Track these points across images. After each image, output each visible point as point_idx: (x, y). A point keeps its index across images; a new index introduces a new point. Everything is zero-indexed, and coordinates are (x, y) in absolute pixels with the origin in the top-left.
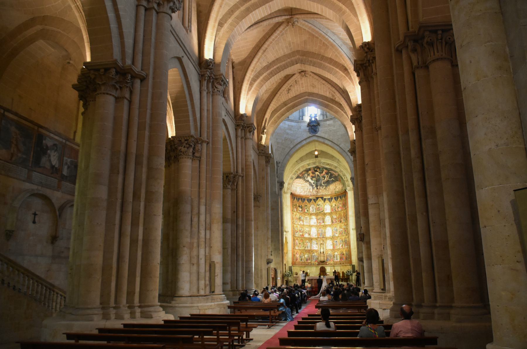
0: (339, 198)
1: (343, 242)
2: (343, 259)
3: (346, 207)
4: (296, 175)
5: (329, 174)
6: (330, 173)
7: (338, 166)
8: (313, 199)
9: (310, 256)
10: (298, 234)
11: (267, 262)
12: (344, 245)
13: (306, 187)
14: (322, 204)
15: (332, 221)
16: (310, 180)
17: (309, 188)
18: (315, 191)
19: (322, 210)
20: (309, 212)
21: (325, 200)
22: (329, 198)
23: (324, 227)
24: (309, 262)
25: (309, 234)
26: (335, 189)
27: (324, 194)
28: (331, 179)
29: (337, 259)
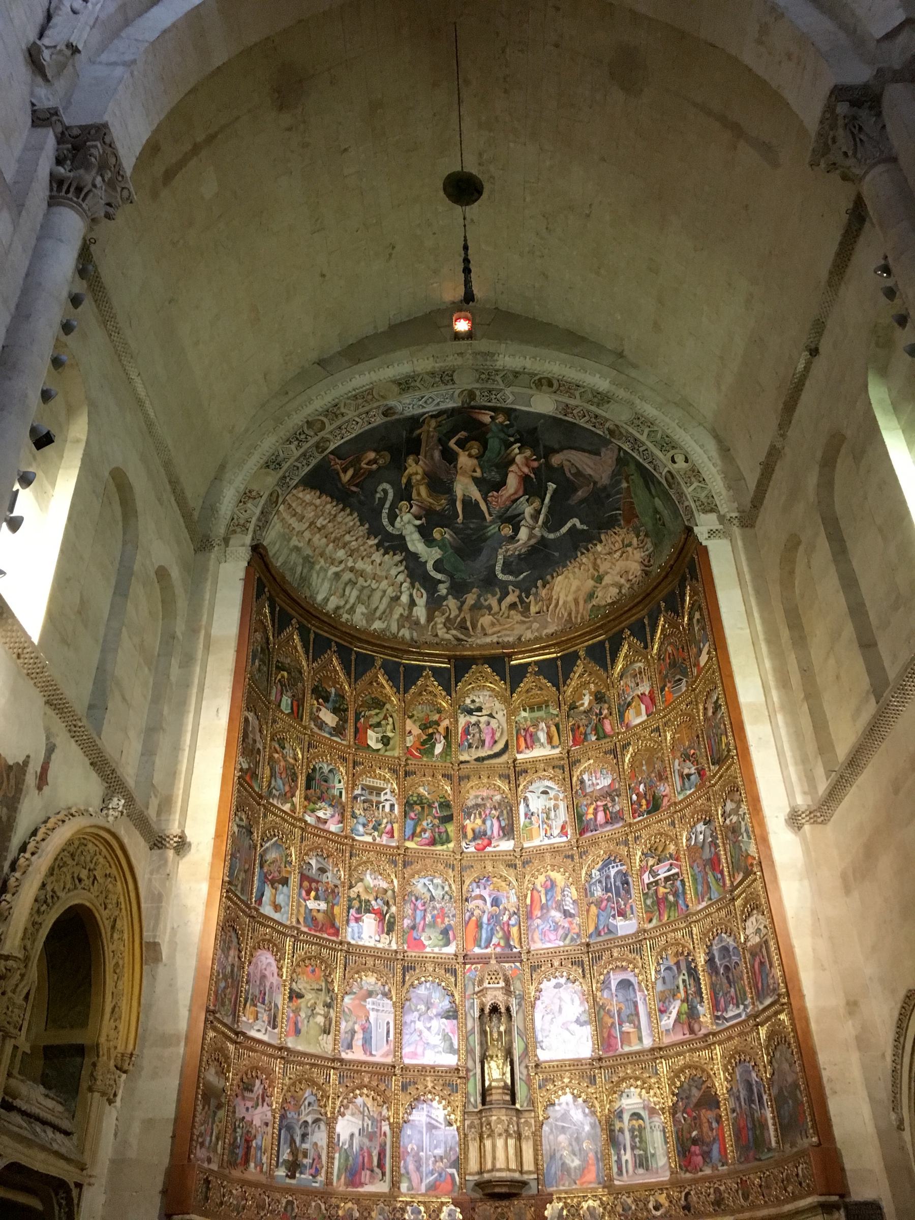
2: (706, 1155)
4: (306, 446)
5: (552, 486)
7: (621, 393)
8: (431, 668)
9: (386, 1128)
12: (704, 1011)
13: (384, 583)
16: (416, 544)
17: (404, 599)
19: (495, 742)
20: (396, 753)
21: (515, 676)
22: (556, 659)
23: (515, 866)
27: (511, 639)
28: (564, 530)
29: (643, 1162)
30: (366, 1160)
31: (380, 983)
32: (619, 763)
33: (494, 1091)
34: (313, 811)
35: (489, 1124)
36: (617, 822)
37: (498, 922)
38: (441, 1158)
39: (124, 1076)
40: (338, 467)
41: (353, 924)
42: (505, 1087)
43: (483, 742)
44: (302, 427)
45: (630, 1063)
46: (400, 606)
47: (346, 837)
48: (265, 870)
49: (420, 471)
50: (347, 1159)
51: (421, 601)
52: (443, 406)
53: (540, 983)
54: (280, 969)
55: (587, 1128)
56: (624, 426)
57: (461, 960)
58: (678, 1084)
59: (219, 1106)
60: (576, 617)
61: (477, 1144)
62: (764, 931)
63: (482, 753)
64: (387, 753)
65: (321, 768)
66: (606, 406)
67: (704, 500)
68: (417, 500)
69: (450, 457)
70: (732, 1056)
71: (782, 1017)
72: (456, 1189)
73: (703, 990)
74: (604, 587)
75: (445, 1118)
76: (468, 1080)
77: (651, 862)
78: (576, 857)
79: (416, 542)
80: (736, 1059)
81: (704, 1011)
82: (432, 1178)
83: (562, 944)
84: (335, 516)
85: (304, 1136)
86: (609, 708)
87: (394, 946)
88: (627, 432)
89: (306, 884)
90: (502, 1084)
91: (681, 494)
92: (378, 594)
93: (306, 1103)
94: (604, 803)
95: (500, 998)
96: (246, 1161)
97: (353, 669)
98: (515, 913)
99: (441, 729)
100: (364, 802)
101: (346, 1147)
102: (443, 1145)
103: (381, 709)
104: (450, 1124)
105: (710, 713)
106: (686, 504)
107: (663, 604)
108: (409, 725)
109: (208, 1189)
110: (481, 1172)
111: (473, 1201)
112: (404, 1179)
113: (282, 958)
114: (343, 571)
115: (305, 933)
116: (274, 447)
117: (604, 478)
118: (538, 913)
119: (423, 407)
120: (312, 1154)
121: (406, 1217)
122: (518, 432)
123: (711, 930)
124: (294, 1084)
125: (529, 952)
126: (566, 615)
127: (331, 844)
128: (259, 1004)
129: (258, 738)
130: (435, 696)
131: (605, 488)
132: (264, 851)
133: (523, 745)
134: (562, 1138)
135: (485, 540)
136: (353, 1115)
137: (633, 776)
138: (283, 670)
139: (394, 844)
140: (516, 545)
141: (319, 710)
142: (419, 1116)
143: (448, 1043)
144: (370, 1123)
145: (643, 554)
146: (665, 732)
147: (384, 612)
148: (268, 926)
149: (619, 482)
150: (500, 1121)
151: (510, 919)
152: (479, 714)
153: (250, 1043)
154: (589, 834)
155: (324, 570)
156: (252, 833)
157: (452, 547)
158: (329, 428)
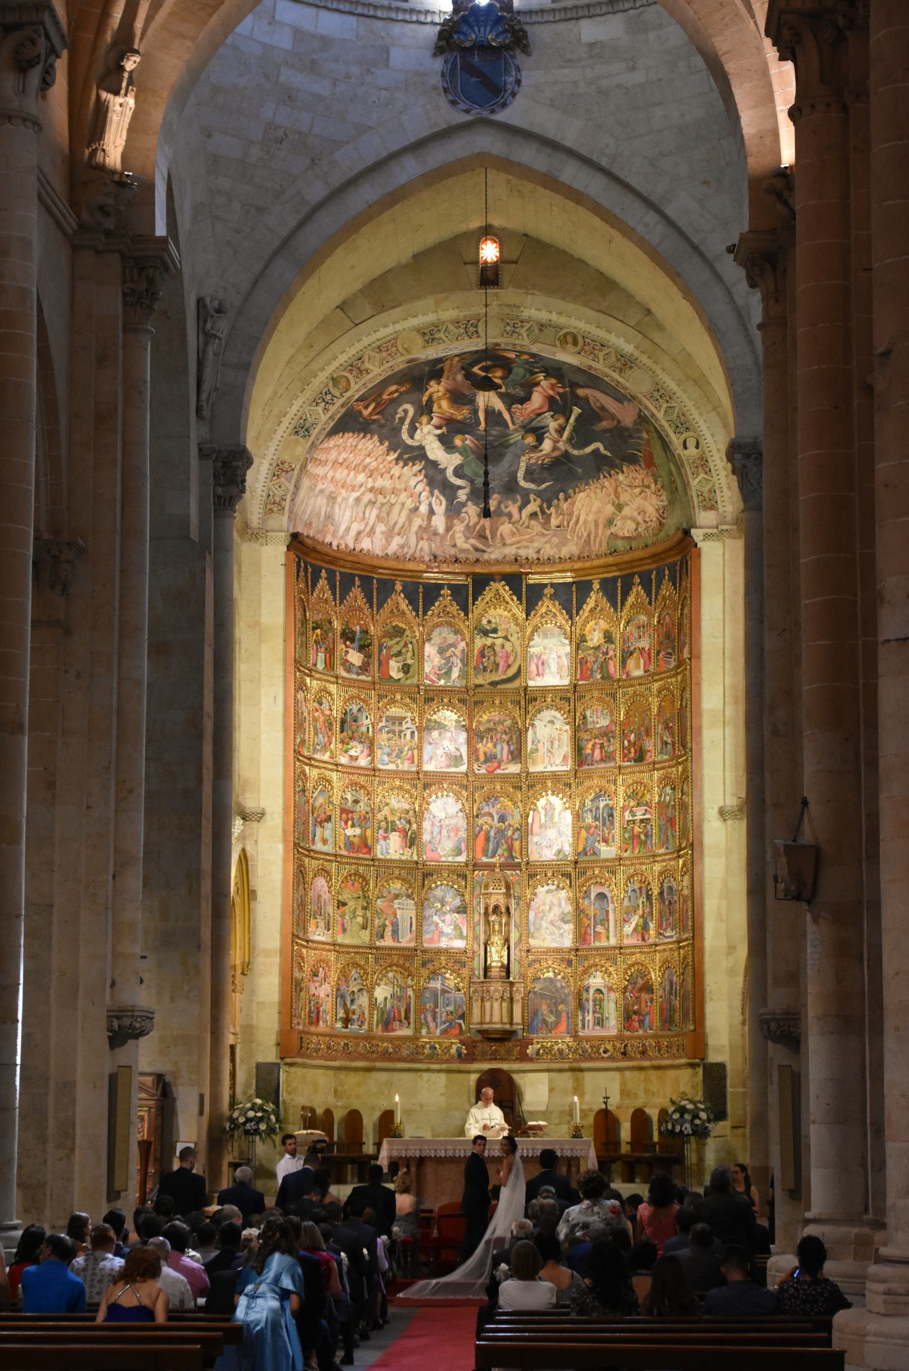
0: (637, 593)
1: (649, 897)
2: (641, 1022)
3: (681, 651)
4: (332, 409)
5: (576, 411)
6: (583, 402)
7: (644, 359)
8: (450, 587)
9: (410, 992)
10: (328, 834)
11: (110, 1029)
13: (403, 496)
14: (513, 628)
15: (578, 748)
16: (435, 451)
17: (424, 509)
19: (509, 666)
20: (414, 681)
22: (570, 585)
25: (412, 840)
26: (610, 522)
28: (588, 450)
29: (600, 1022)
32: (618, 707)
34: (346, 752)
35: (488, 992)
38: (452, 1012)
41: (382, 842)
42: (502, 966)
43: (497, 665)
46: (418, 516)
47: (374, 770)
48: (315, 815)
50: (383, 1013)
51: (440, 508)
57: (471, 868)
59: (301, 990)
60: (595, 540)
63: (496, 677)
64: (408, 682)
66: (629, 372)
67: (706, 495)
74: (623, 518)
77: (632, 803)
78: (573, 786)
79: (436, 450)
80: (666, 965)
82: (444, 1026)
84: (356, 446)
85: (352, 1001)
86: (614, 650)
87: (415, 858)
89: (344, 816)
90: (499, 964)
91: (689, 482)
92: (396, 509)
95: (501, 901)
96: (318, 1021)
100: (388, 733)
102: (453, 1003)
103: (401, 637)
104: (459, 990)
107: (667, 572)
109: (302, 1042)
112: (424, 1027)
113: (331, 880)
114: (363, 494)
116: (301, 410)
118: (536, 828)
120: (358, 1012)
123: (664, 872)
124: (344, 967)
126: (585, 535)
127: (363, 778)
129: (304, 708)
130: (454, 617)
131: (627, 429)
136: (386, 984)
138: (317, 628)
139: (414, 769)
140: (540, 454)
141: (347, 652)
143: (458, 932)
147: (403, 527)
149: (639, 431)
150: (496, 990)
154: (586, 767)
155: (345, 499)
157: (473, 452)
158: (354, 387)
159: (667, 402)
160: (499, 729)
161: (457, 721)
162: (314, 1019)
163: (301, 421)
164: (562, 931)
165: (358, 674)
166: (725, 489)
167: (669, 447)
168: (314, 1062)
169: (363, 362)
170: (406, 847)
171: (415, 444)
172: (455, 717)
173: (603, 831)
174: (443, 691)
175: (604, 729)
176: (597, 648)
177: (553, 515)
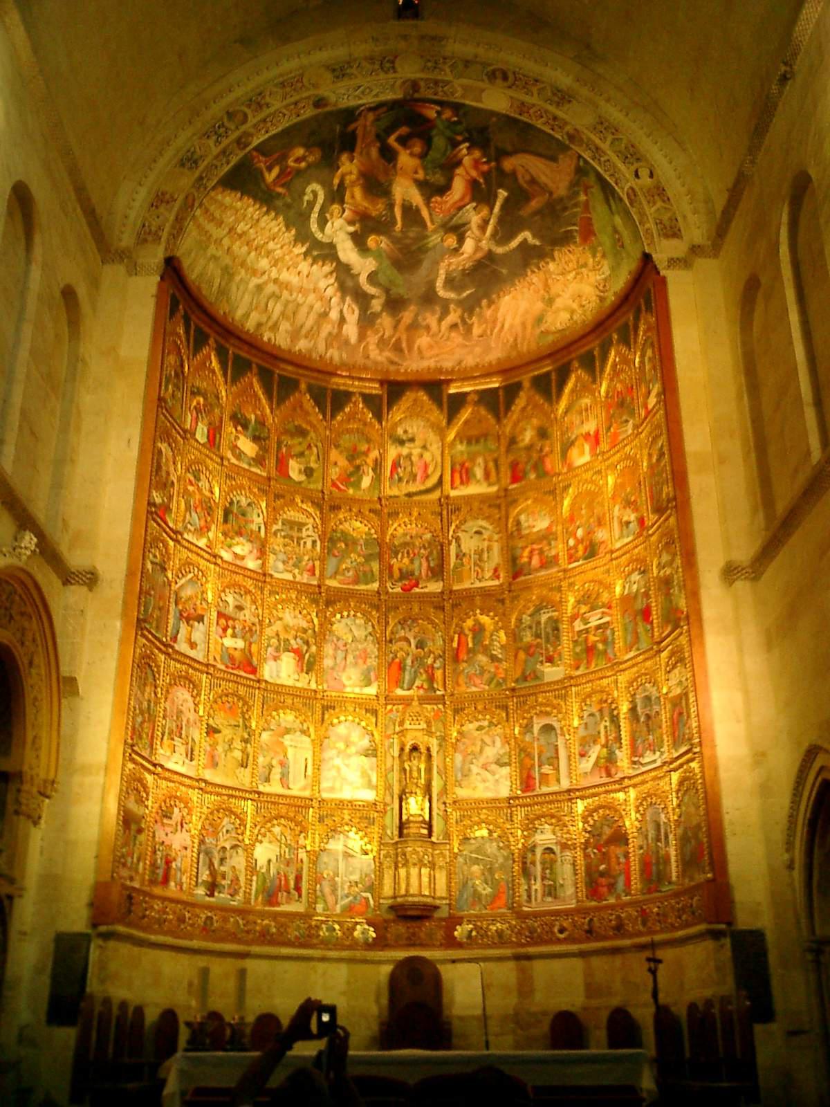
2: (611, 887)
4: (225, 142)
5: (503, 194)
12: (623, 756)
13: (311, 298)
16: (347, 252)
17: (334, 315)
18: (382, 343)
19: (427, 477)
24: (292, 916)
28: (514, 244)
29: (551, 891)
30: (283, 883)
31: (298, 721)
33: (411, 825)
34: (230, 546)
35: (404, 854)
36: (552, 567)
37: (422, 664)
39: (47, 801)
40: (262, 165)
42: (424, 822)
43: (415, 476)
44: (222, 119)
45: (547, 802)
47: (264, 575)
48: (180, 607)
49: (355, 171)
50: (264, 880)
51: (352, 317)
52: (383, 98)
53: (462, 725)
54: (196, 705)
55: (501, 860)
56: (586, 131)
57: (382, 701)
58: (591, 822)
59: (140, 831)
60: (522, 344)
61: (391, 872)
62: (685, 684)
63: (413, 488)
64: (312, 486)
65: (238, 502)
66: (567, 106)
67: (667, 223)
68: (350, 204)
69: (389, 155)
70: (645, 799)
71: (694, 765)
72: (370, 910)
73: (623, 736)
74: (555, 312)
75: (362, 849)
76: (386, 812)
77: (584, 609)
78: (507, 602)
81: (623, 756)
82: (347, 901)
83: (487, 687)
84: (258, 220)
85: (222, 860)
87: (313, 686)
88: (589, 139)
89: (223, 621)
90: (421, 819)
91: (642, 214)
92: (304, 310)
93: (224, 830)
94: (540, 546)
95: (422, 740)
96: (166, 880)
97: (275, 393)
98: (440, 656)
99: (370, 460)
100: (284, 537)
101: (264, 870)
102: (358, 873)
105: (654, 460)
106: (647, 226)
107: (615, 336)
108: (334, 454)
109: (131, 904)
110: (395, 897)
111: (386, 921)
113: (199, 694)
114: (266, 283)
115: (221, 670)
117: (561, 190)
118: (463, 656)
119: (360, 98)
120: (230, 875)
121: (321, 933)
122: (468, 130)
123: (636, 680)
124: (212, 813)
125: (452, 695)
126: (512, 340)
127: (250, 582)
128: (176, 738)
130: (365, 424)
131: (561, 200)
132: (179, 588)
133: (457, 481)
134: (475, 868)
135: (426, 252)
136: (270, 842)
137: (572, 519)
139: (315, 583)
141: (237, 438)
142: (336, 845)
144: (287, 850)
145: (598, 277)
146: (607, 476)
148: (184, 664)
149: (576, 194)
151: (434, 662)
152: (412, 445)
153: (167, 774)
154: (522, 578)
156: (164, 569)
157: (389, 257)
158: (252, 120)
159: (613, 134)
160: (417, 544)
161: (368, 534)
162: (160, 878)
163: (189, 154)
164: (497, 777)
165: (250, 465)
166: (689, 215)
167: (613, 192)
168: (153, 938)
169: (264, 97)
170: (302, 670)
171: (326, 240)
172: (367, 529)
173: (547, 649)
174: (353, 500)
175: (541, 534)
176: (530, 448)
177: (476, 326)
